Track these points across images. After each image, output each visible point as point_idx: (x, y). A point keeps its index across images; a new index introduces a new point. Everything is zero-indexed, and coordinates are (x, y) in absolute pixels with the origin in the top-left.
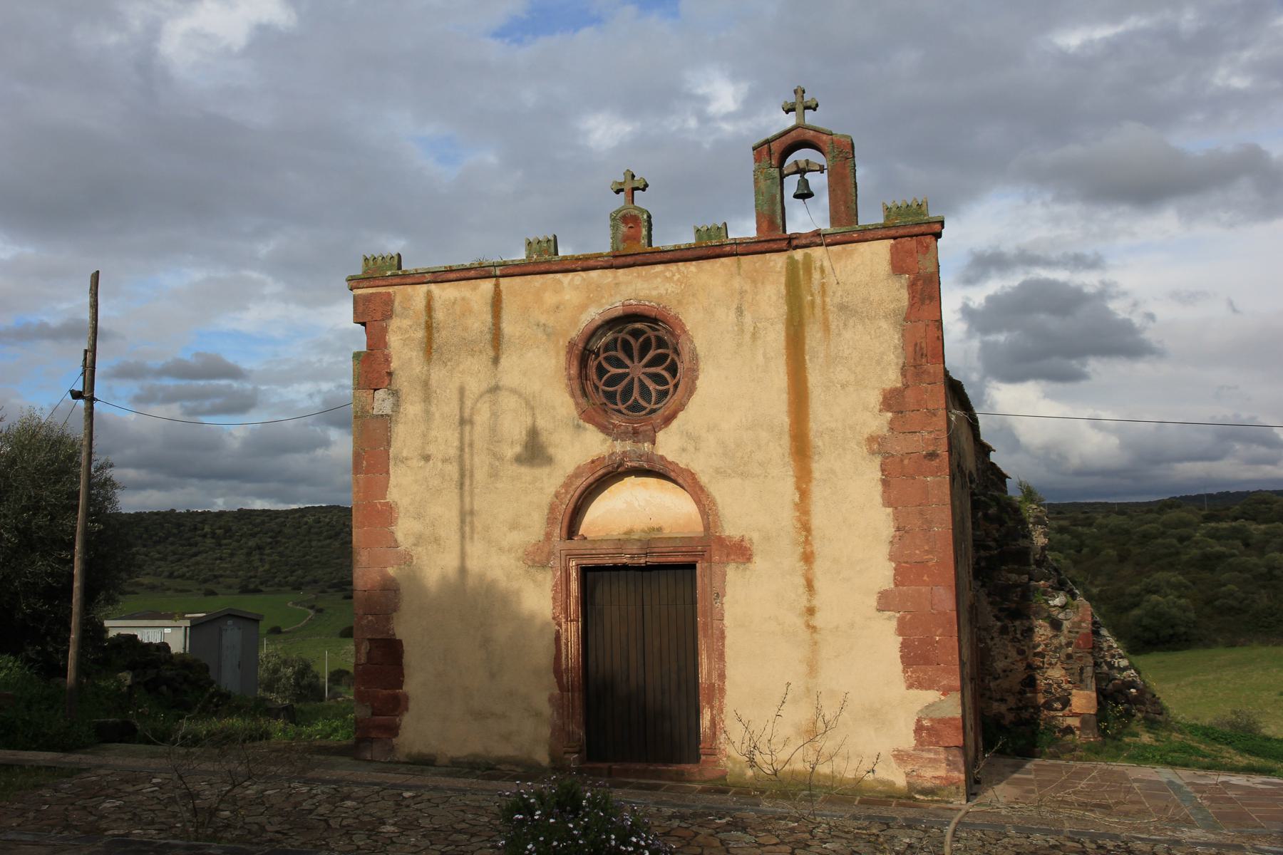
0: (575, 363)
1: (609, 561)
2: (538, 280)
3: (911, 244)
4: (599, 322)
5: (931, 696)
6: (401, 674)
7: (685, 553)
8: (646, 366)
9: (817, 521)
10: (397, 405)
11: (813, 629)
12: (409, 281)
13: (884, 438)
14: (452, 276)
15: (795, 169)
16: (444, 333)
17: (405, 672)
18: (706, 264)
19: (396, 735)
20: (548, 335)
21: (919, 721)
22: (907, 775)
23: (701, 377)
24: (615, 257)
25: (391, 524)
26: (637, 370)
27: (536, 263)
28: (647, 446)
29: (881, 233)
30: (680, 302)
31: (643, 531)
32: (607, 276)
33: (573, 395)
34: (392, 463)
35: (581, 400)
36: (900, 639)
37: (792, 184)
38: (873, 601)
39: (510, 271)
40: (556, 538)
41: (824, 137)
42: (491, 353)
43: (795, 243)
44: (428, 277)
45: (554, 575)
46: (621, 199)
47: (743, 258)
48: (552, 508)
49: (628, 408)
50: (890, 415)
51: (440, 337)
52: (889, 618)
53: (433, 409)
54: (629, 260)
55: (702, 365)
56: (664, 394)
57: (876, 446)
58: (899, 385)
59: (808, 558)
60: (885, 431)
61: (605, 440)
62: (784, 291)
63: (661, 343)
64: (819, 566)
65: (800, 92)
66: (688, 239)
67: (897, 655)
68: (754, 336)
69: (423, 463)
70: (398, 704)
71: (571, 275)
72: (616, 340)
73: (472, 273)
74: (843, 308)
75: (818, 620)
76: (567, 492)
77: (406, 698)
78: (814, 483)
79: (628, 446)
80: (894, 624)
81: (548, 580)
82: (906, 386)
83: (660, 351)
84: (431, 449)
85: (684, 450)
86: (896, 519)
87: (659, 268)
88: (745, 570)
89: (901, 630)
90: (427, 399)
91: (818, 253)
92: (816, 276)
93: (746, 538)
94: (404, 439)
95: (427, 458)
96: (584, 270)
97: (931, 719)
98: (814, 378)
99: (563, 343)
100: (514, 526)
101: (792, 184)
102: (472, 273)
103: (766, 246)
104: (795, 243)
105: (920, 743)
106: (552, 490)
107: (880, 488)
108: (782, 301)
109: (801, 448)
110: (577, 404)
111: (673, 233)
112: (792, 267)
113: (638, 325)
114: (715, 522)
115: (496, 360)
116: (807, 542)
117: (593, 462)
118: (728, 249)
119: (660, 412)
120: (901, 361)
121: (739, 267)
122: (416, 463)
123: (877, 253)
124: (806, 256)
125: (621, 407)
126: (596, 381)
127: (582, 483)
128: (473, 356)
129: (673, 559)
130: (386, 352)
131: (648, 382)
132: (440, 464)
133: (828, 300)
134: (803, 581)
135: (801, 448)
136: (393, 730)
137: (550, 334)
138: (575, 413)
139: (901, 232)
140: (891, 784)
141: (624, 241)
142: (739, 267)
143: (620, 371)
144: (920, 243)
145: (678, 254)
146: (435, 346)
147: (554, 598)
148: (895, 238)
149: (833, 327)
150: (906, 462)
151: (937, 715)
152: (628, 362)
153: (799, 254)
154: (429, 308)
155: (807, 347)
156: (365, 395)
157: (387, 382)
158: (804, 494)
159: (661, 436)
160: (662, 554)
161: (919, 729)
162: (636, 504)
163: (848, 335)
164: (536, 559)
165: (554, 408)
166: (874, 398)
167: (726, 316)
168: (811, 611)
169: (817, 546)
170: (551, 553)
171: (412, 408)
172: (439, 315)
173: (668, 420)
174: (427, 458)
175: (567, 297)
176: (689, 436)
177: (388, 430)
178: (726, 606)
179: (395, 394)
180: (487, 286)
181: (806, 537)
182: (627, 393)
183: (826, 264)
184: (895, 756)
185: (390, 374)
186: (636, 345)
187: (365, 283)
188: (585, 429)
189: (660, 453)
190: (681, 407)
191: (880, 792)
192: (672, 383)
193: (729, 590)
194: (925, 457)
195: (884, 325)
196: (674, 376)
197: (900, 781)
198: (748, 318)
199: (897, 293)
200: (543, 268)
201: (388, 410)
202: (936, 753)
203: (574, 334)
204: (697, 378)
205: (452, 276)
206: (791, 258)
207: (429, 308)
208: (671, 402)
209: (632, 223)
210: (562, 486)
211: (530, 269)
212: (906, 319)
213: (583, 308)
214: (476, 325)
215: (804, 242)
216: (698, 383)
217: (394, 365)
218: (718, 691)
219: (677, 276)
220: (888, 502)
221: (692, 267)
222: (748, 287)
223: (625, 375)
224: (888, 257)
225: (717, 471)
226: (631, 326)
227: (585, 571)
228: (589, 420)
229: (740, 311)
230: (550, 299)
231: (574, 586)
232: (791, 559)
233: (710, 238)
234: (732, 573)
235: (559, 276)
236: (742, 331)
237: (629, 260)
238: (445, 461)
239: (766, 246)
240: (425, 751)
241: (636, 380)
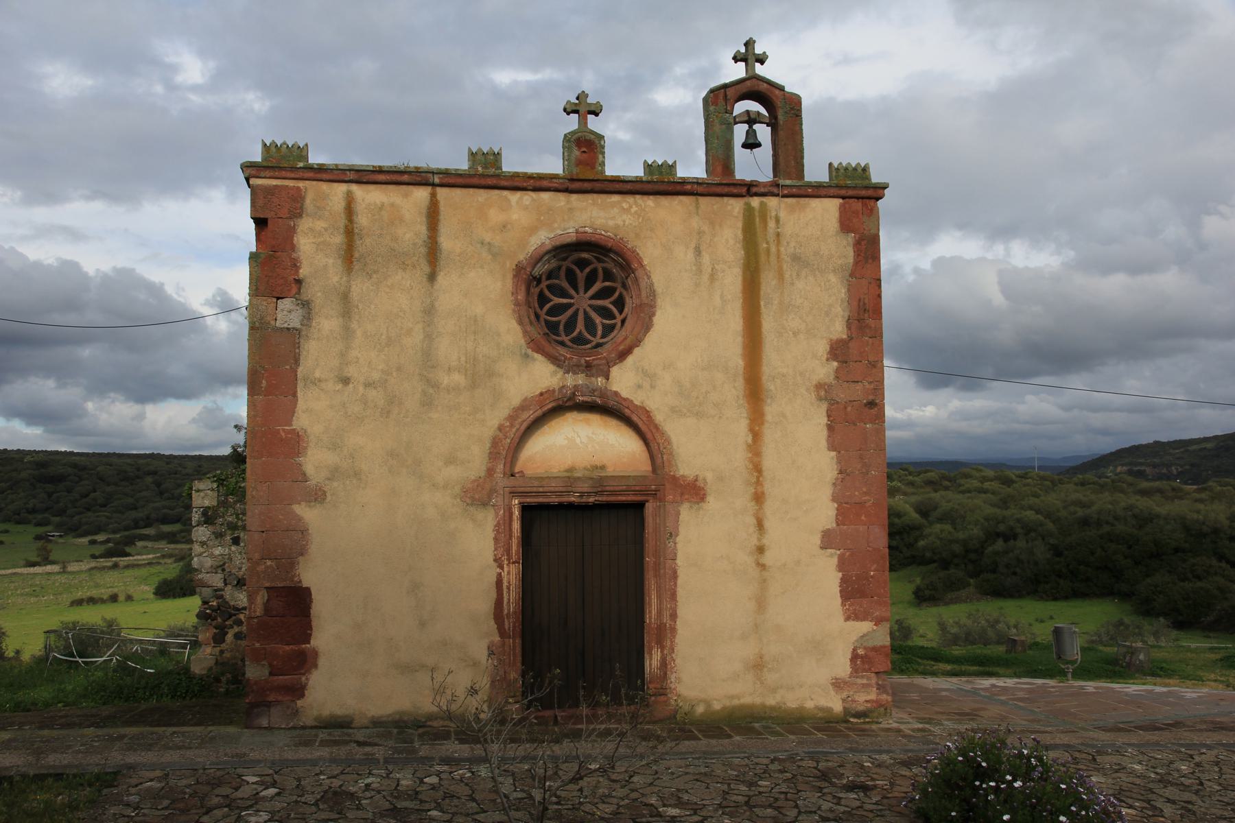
0: (523, 288)
1: (554, 500)
2: (482, 195)
3: (857, 205)
4: (549, 247)
5: (866, 626)
6: (309, 626)
7: (637, 492)
8: (592, 298)
9: (768, 462)
10: (308, 318)
11: (763, 567)
12: (324, 176)
13: (830, 386)
14: (382, 177)
15: (746, 118)
16: (368, 241)
17: (314, 624)
18: (665, 201)
19: (302, 696)
20: (494, 255)
21: (854, 650)
22: (844, 700)
23: (658, 313)
24: (572, 180)
25: (298, 454)
26: (582, 301)
27: (483, 176)
28: (600, 381)
29: (832, 191)
30: (637, 235)
31: (585, 469)
32: (560, 201)
33: (520, 322)
34: (300, 385)
35: (529, 328)
36: (840, 575)
37: (740, 131)
38: (817, 540)
39: (451, 181)
40: (499, 475)
41: (777, 92)
42: (427, 269)
43: (754, 190)
44: (352, 176)
45: (497, 514)
46: (572, 122)
47: (702, 200)
48: (495, 443)
49: (574, 341)
50: (835, 364)
51: (362, 246)
52: (831, 555)
53: (354, 325)
54: (587, 185)
55: (659, 302)
56: (609, 329)
57: (823, 393)
58: (845, 337)
59: (759, 498)
60: (831, 379)
61: (555, 373)
62: (740, 236)
63: (608, 276)
64: (770, 507)
65: (749, 44)
66: (635, 170)
67: (836, 589)
68: (713, 277)
69: (340, 386)
70: (304, 661)
71: (519, 194)
72: (559, 268)
73: (405, 178)
74: (796, 258)
75: (768, 558)
76: (512, 426)
77: (315, 654)
78: (766, 425)
79: (580, 379)
80: (835, 561)
81: (488, 520)
82: (851, 338)
83: (607, 284)
84: (351, 371)
85: (640, 387)
86: (839, 462)
87: (615, 198)
88: (699, 509)
89: (841, 566)
91: (772, 202)
92: (772, 224)
93: (700, 478)
94: (316, 357)
95: (346, 381)
96: (535, 189)
97: (865, 648)
98: (768, 324)
99: (510, 265)
100: (451, 460)
101: (740, 131)
102: (405, 178)
103: (726, 190)
104: (754, 190)
105: (855, 671)
106: (495, 423)
107: (825, 433)
108: (739, 245)
109: (755, 392)
110: (525, 332)
111: (617, 165)
112: (749, 213)
113: (585, 255)
114: (669, 462)
115: (432, 277)
116: (758, 483)
117: (541, 394)
118: (689, 187)
119: (606, 346)
120: (846, 314)
121: (697, 207)
122: (330, 386)
123: (827, 210)
124: (762, 204)
125: (566, 339)
126: (538, 310)
127: (529, 416)
128: (404, 270)
129: (624, 498)
130: (294, 255)
131: (594, 315)
132: (361, 389)
133: (782, 249)
134: (753, 521)
135: (755, 392)
136: (299, 691)
137: (496, 254)
138: (522, 342)
139: (850, 193)
140: (829, 710)
141: (577, 165)
142: (697, 207)
143: (565, 301)
144: (864, 205)
145: (638, 187)
146: (356, 255)
147: (496, 539)
148: (843, 198)
149: (787, 276)
150: (849, 409)
151: (870, 644)
152: (573, 292)
153: (755, 202)
154: (350, 211)
155: (762, 293)
156: (265, 303)
157: (294, 290)
158: (756, 435)
159: (615, 371)
160: (614, 493)
161: (855, 657)
162: (578, 441)
163: (800, 285)
164: (476, 496)
165: (499, 335)
166: (822, 348)
167: (684, 255)
168: (761, 550)
169: (767, 487)
170: (492, 491)
171: (327, 323)
172: (362, 220)
173: (623, 355)
174: (346, 381)
175: (515, 217)
176: (645, 373)
178: (679, 546)
179: (306, 305)
180: (421, 195)
181: (758, 478)
182: (570, 325)
183: (782, 215)
184: (833, 684)
185: (299, 282)
186: (581, 276)
187: (267, 173)
188: (534, 360)
189: (614, 389)
190: (637, 343)
191: (821, 718)
192: (619, 318)
193: (682, 530)
194: (866, 405)
195: (833, 279)
196: (621, 312)
197: (837, 706)
198: (706, 259)
199: (842, 250)
200: (489, 182)
201: (298, 325)
202: (869, 678)
203: (521, 257)
204: (654, 314)
205: (382, 177)
206: (748, 204)
207: (350, 211)
208: (619, 335)
209: (585, 147)
210: (507, 419)
211: (475, 181)
212: (851, 275)
213: (533, 230)
214: (408, 236)
215: (762, 190)
216: (656, 319)
217: (304, 272)
218: (665, 633)
219: (634, 209)
220: (832, 447)
221: (649, 202)
222: (705, 228)
223: (570, 306)
224: (837, 215)
225: (673, 410)
226: (576, 256)
227: (526, 509)
228: (539, 349)
229: (698, 251)
230: (495, 216)
231: (516, 526)
232: (743, 500)
233: (661, 173)
234: (686, 513)
235: (505, 193)
236: (699, 271)
237: (587, 185)
238: (368, 385)
239: (726, 190)
240: (339, 712)
241: (588, 309)
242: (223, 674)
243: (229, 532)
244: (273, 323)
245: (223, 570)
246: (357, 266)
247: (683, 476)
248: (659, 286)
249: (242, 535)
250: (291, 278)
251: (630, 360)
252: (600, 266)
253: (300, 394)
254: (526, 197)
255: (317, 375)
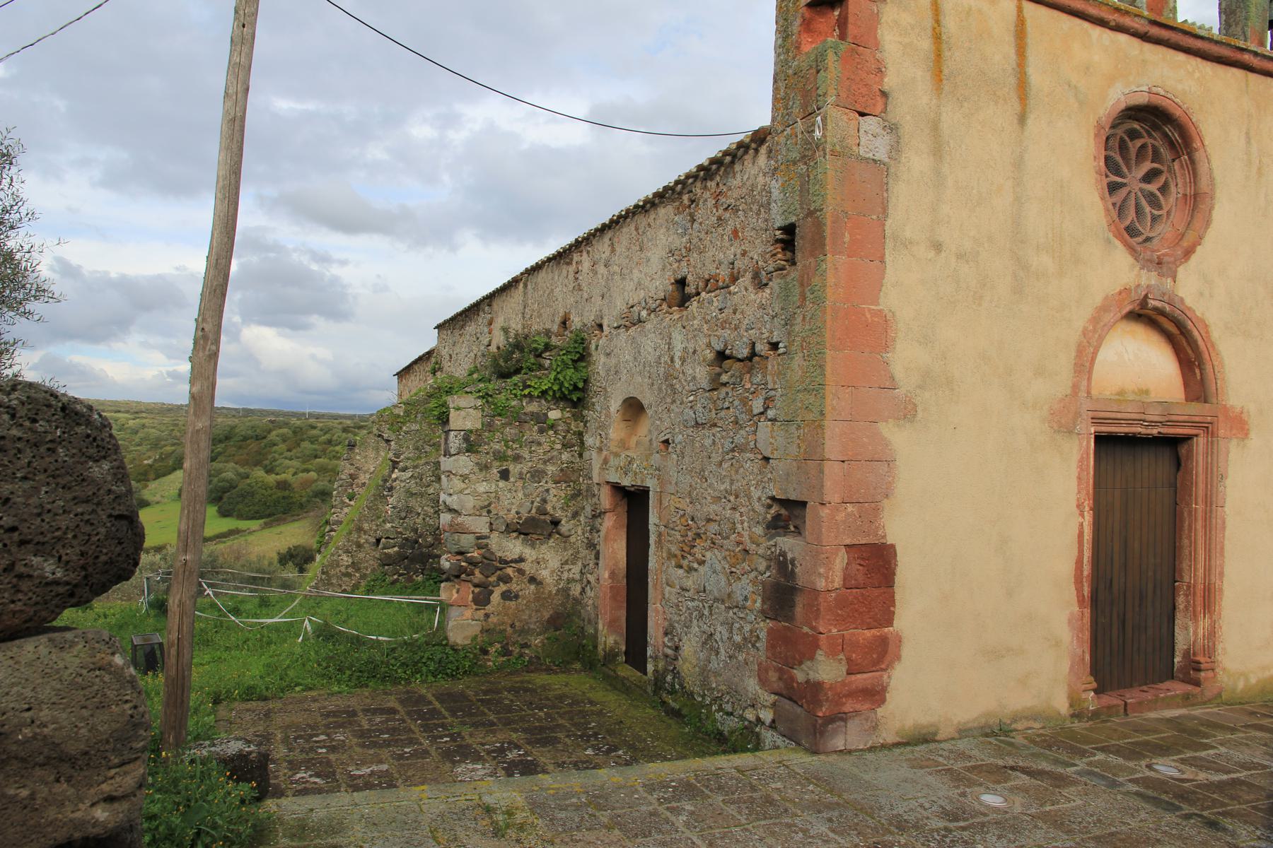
6: (891, 601)
10: (896, 149)
17: (897, 597)
19: (883, 701)
25: (886, 348)
31: (1133, 392)
45: (1081, 444)
51: (954, 59)
55: (1218, 194)
69: (932, 254)
70: (882, 653)
77: (899, 640)
83: (1155, 165)
87: (1181, 57)
90: (938, 151)
95: (938, 247)
99: (1092, 121)
115: (1022, 119)
117: (1120, 293)
130: (878, 55)
136: (876, 695)
143: (1119, 180)
146: (946, 71)
147: (1079, 478)
170: (1077, 414)
171: (916, 161)
174: (938, 247)
177: (885, 187)
179: (892, 129)
185: (884, 94)
210: (1090, 321)
217: (889, 82)
218: (1209, 599)
238: (960, 256)
242: (491, 644)
243: (496, 464)
244: (855, 148)
245: (489, 512)
246: (947, 87)
247: (1232, 407)
248: (1217, 174)
249: (511, 468)
250: (876, 88)
251: (1194, 258)
252: (1150, 141)
253: (888, 259)
254: (1105, 36)
255: (908, 234)
